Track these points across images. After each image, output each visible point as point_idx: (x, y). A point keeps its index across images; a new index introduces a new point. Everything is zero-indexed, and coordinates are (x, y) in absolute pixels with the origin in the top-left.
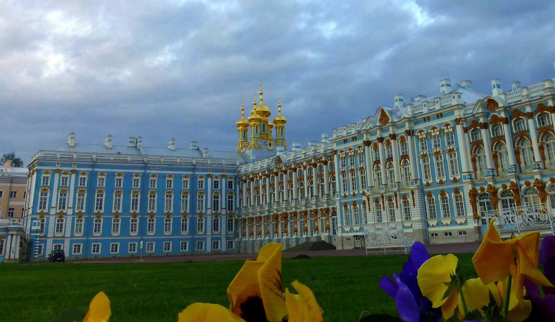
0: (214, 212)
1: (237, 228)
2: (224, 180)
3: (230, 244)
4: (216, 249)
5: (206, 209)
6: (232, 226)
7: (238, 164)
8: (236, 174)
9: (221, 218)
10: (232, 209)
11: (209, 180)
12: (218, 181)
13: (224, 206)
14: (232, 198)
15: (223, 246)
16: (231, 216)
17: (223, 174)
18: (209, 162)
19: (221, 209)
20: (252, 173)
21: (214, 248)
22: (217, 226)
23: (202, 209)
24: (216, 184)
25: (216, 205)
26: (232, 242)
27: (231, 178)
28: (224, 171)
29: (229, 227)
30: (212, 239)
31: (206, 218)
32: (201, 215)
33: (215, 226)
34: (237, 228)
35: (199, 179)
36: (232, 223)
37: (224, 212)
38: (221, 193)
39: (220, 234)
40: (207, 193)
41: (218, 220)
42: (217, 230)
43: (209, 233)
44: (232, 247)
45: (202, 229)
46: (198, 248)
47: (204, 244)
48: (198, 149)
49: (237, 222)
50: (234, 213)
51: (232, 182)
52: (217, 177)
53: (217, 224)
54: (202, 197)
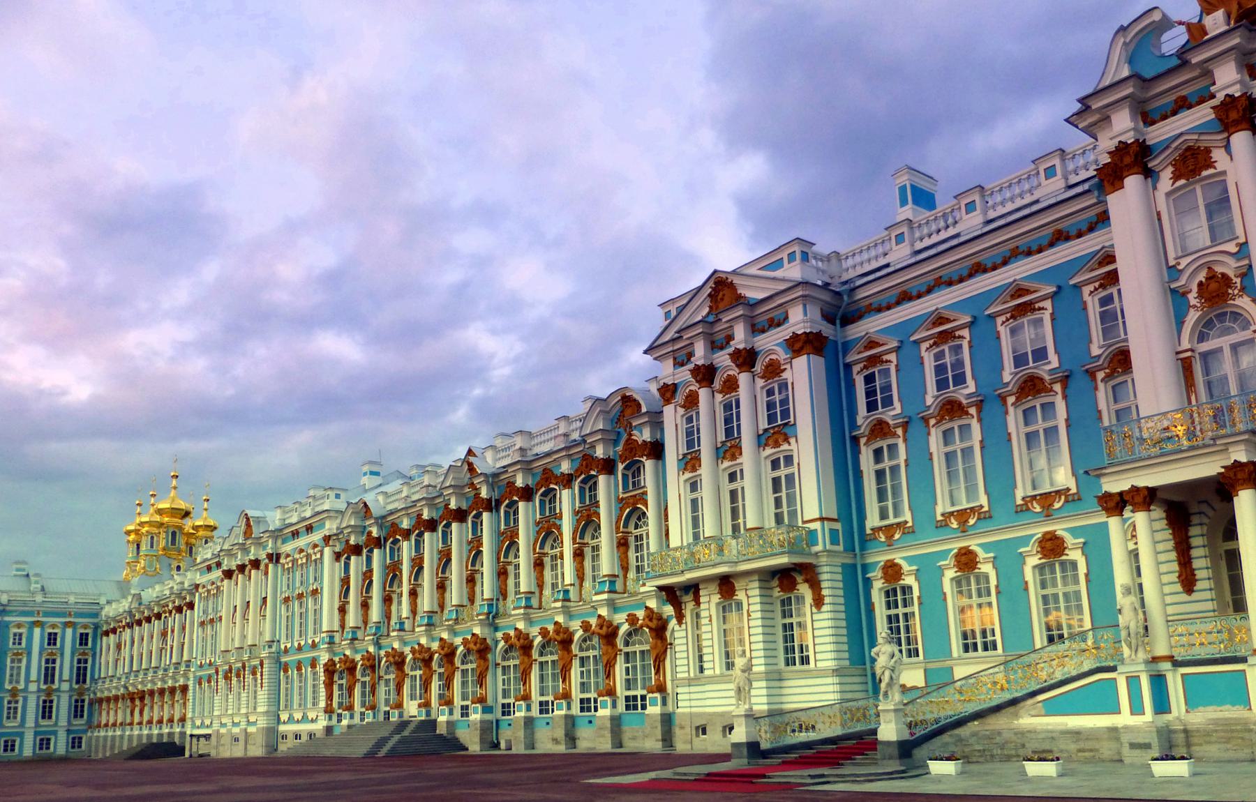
0: (43, 687)
1: (91, 714)
2: (69, 631)
3: (76, 742)
4: (44, 751)
5: (28, 681)
6: (82, 711)
7: (103, 601)
8: (95, 620)
9: (59, 697)
10: (84, 681)
11: (37, 631)
12: (56, 634)
13: (66, 676)
14: (86, 661)
15: (60, 746)
16: (81, 694)
17: (68, 620)
18: (39, 598)
19: (61, 680)
20: (114, 619)
21: (41, 748)
22: (50, 712)
23: (18, 682)
24: (52, 639)
25: (49, 675)
26: (80, 738)
27: (85, 627)
28: (70, 615)
29: (77, 711)
30: (36, 734)
31: (25, 699)
32: (14, 693)
33: (46, 710)
34: (91, 714)
35: (16, 630)
36: (83, 707)
37: (65, 686)
38: (62, 655)
39: (56, 724)
40: (29, 654)
41: (51, 702)
42: (50, 717)
43: (30, 722)
44: (80, 747)
45: (15, 718)
46: (5, 750)
47: (17, 744)
48: (28, 575)
49: (91, 704)
50: (88, 689)
51: (87, 634)
52: (53, 626)
53: (51, 707)
54: (20, 661)
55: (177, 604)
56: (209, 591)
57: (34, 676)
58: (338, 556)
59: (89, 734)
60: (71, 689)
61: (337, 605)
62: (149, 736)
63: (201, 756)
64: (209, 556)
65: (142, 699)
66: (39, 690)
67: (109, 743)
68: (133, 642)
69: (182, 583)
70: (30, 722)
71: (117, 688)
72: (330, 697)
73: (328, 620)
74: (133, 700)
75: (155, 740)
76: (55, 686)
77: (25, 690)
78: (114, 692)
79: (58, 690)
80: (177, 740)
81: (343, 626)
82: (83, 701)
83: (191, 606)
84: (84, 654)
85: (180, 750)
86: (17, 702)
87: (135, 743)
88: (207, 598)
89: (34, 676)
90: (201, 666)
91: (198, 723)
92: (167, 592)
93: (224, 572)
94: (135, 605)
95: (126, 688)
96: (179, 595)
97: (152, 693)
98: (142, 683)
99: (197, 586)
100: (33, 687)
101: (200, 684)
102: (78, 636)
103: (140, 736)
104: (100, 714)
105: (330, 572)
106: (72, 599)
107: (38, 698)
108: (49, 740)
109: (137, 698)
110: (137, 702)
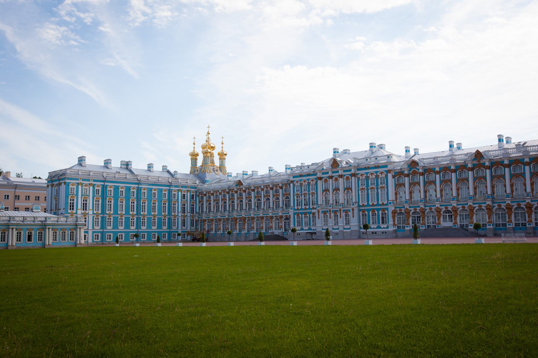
2: (189, 193)
11: (180, 193)
13: (189, 211)
16: (193, 218)
24: (184, 196)
25: (184, 211)
31: (178, 218)
32: (175, 216)
34: (196, 225)
37: (189, 215)
43: (180, 228)
49: (196, 222)
57: (180, 211)
58: (394, 177)
61: (394, 192)
70: (180, 228)
72: (394, 221)
73: (392, 197)
77: (178, 215)
79: (187, 216)
81: (396, 199)
89: (180, 211)
99: (292, 182)
105: (391, 182)
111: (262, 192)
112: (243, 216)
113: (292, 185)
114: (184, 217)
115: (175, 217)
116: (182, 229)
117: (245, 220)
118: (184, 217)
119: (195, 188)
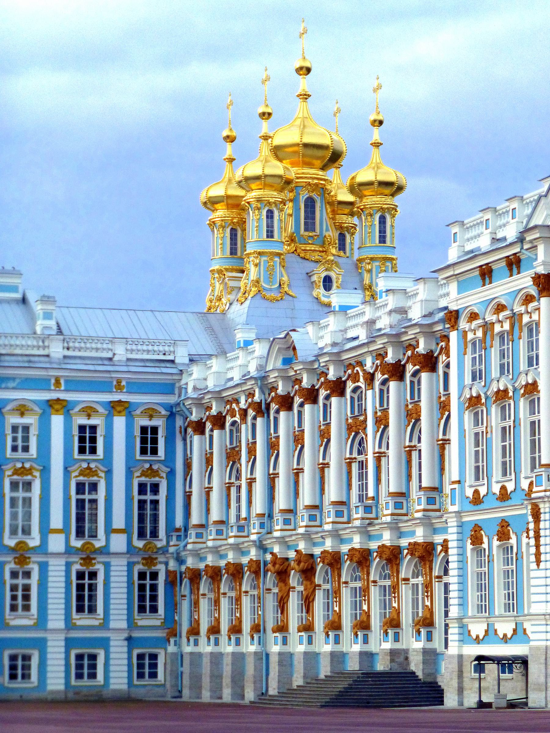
0: (78, 544)
1: (173, 606)
2: (119, 423)
3: (145, 665)
4: (86, 682)
5: (46, 530)
6: (154, 598)
7: (181, 357)
8: (172, 399)
9: (107, 565)
10: (155, 534)
11: (57, 422)
12: (94, 428)
13: (119, 522)
14: (155, 488)
15: (116, 673)
16: (150, 561)
17: (116, 397)
18: (57, 350)
19: (110, 530)
20: (218, 395)
21: (79, 676)
22: (92, 598)
23: (27, 531)
24: (87, 439)
25: (83, 518)
26: (154, 657)
27: (151, 413)
28: (119, 387)
29: (144, 598)
30: (69, 643)
31: (44, 568)
32: (22, 554)
33: (84, 595)
35: (14, 420)
36: (154, 588)
37: (119, 543)
38: (109, 473)
39: (104, 625)
40: (46, 471)
41: (93, 575)
42: (92, 610)
43: (56, 620)
44: (153, 675)
45: (27, 608)
46: (13, 677)
47: (34, 662)
48: (24, 300)
49: (172, 581)
50: (164, 550)
51: (155, 430)
52: (89, 411)
53: (93, 588)
54: (28, 486)
55: (390, 358)
56: (487, 327)
57: (56, 520)
59: (171, 648)
60: (131, 550)
62: (367, 657)
63: (512, 705)
64: (484, 243)
65: (308, 572)
66: (69, 550)
67: (227, 670)
68: (273, 446)
69: (402, 311)
71: (238, 549)
74: (282, 575)
75: (381, 666)
76: (99, 543)
78: (231, 557)
80: (416, 666)
82: (154, 576)
83: (429, 362)
84: (155, 473)
85: (433, 693)
86: (27, 574)
87: (324, 670)
88: (483, 344)
89: (56, 520)
90: (477, 500)
91: (478, 629)
92: (363, 335)
93: (537, 279)
94: (275, 363)
95: (262, 547)
96: (395, 338)
97: (334, 561)
98: (307, 537)
99: (453, 317)
100: (56, 543)
101: (477, 540)
102: (137, 433)
103: (311, 658)
104: (196, 604)
106: (121, 352)
107: (68, 565)
108: (93, 657)
109: (297, 573)
110: (294, 579)
111: (369, 393)
112: (302, 546)
113: (454, 336)
114: (87, 560)
115: (22, 560)
116: (70, 625)
117: (282, 575)
118: (87, 560)
119: (169, 388)
